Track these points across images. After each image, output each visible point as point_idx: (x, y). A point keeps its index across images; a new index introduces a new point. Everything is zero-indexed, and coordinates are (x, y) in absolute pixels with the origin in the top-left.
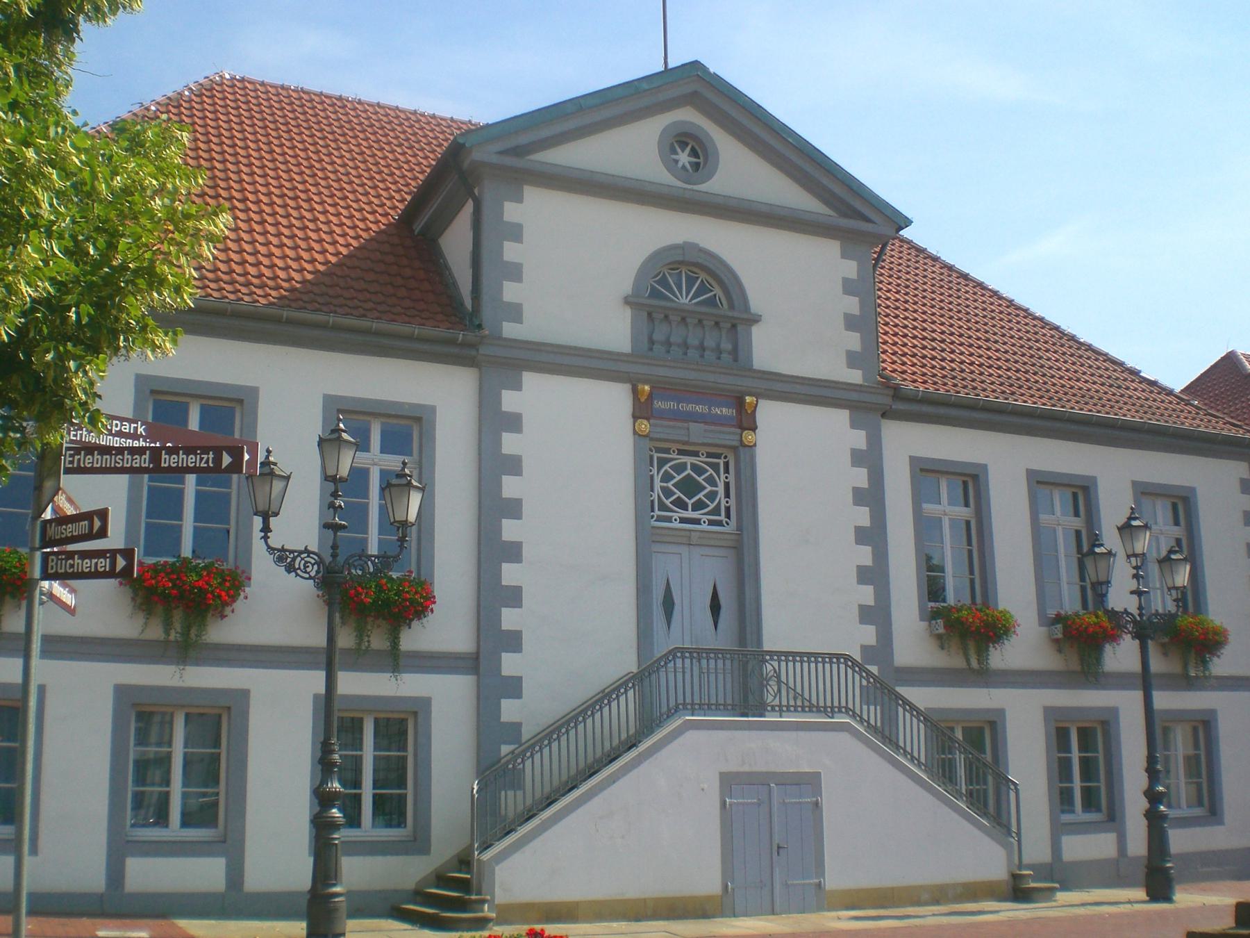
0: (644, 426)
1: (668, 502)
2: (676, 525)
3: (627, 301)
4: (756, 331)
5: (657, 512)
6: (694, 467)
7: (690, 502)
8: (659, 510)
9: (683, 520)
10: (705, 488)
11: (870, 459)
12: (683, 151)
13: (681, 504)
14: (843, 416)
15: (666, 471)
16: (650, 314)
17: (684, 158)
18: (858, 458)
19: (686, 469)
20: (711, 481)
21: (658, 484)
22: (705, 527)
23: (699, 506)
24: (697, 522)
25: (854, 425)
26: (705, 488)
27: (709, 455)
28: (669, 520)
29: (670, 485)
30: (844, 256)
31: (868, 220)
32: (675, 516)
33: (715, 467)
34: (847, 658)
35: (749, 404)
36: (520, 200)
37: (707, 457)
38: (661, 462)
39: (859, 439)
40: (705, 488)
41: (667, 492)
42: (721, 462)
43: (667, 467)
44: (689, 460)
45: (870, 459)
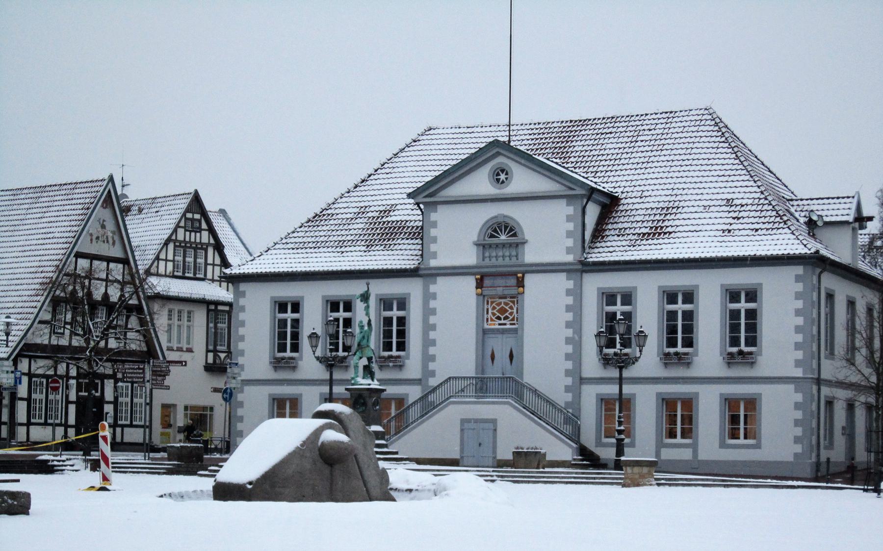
0: (479, 290)
3: (477, 244)
4: (526, 246)
7: (502, 317)
9: (500, 324)
11: (577, 293)
13: (499, 318)
14: (563, 276)
16: (484, 247)
17: (502, 177)
18: (569, 292)
20: (511, 308)
22: (508, 326)
23: (506, 318)
24: (505, 324)
25: (568, 279)
27: (511, 298)
28: (494, 324)
30: (568, 205)
31: (574, 189)
33: (513, 302)
34: (450, 378)
36: (436, 211)
38: (492, 303)
39: (570, 284)
40: (508, 311)
43: (494, 305)
44: (503, 301)
45: (577, 293)
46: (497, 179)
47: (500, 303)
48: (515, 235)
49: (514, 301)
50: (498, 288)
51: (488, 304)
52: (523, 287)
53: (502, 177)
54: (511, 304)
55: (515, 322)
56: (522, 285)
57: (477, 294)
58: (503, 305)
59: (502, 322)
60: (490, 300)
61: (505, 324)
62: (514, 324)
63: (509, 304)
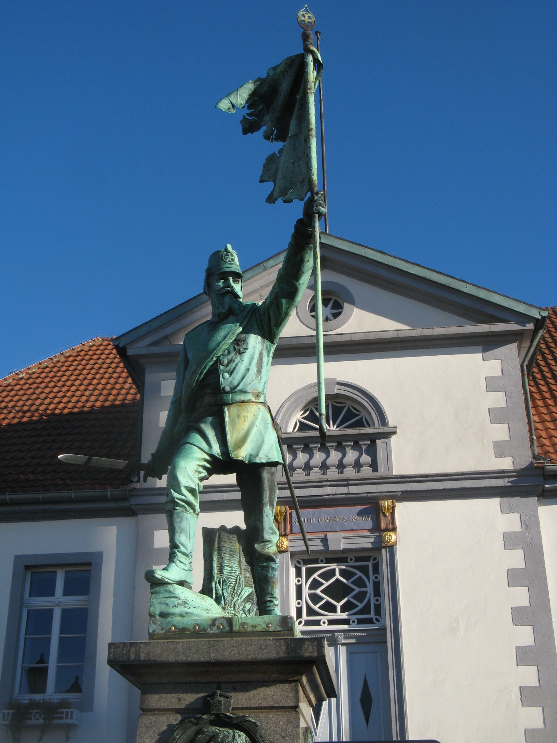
1: (316, 608)
2: (325, 627)
5: (305, 617)
6: (342, 573)
7: (339, 605)
8: (370, 613)
9: (331, 622)
12: (332, 308)
15: (315, 580)
19: (334, 575)
20: (360, 583)
21: (306, 592)
26: (353, 590)
27: (357, 559)
28: (317, 623)
29: (318, 591)
32: (323, 619)
33: (364, 570)
37: (355, 561)
38: (310, 572)
41: (315, 598)
42: (370, 564)
43: (315, 576)
46: (312, 316)
47: (332, 573)
48: (360, 424)
52: (394, 529)
58: (338, 576)
63: (354, 574)
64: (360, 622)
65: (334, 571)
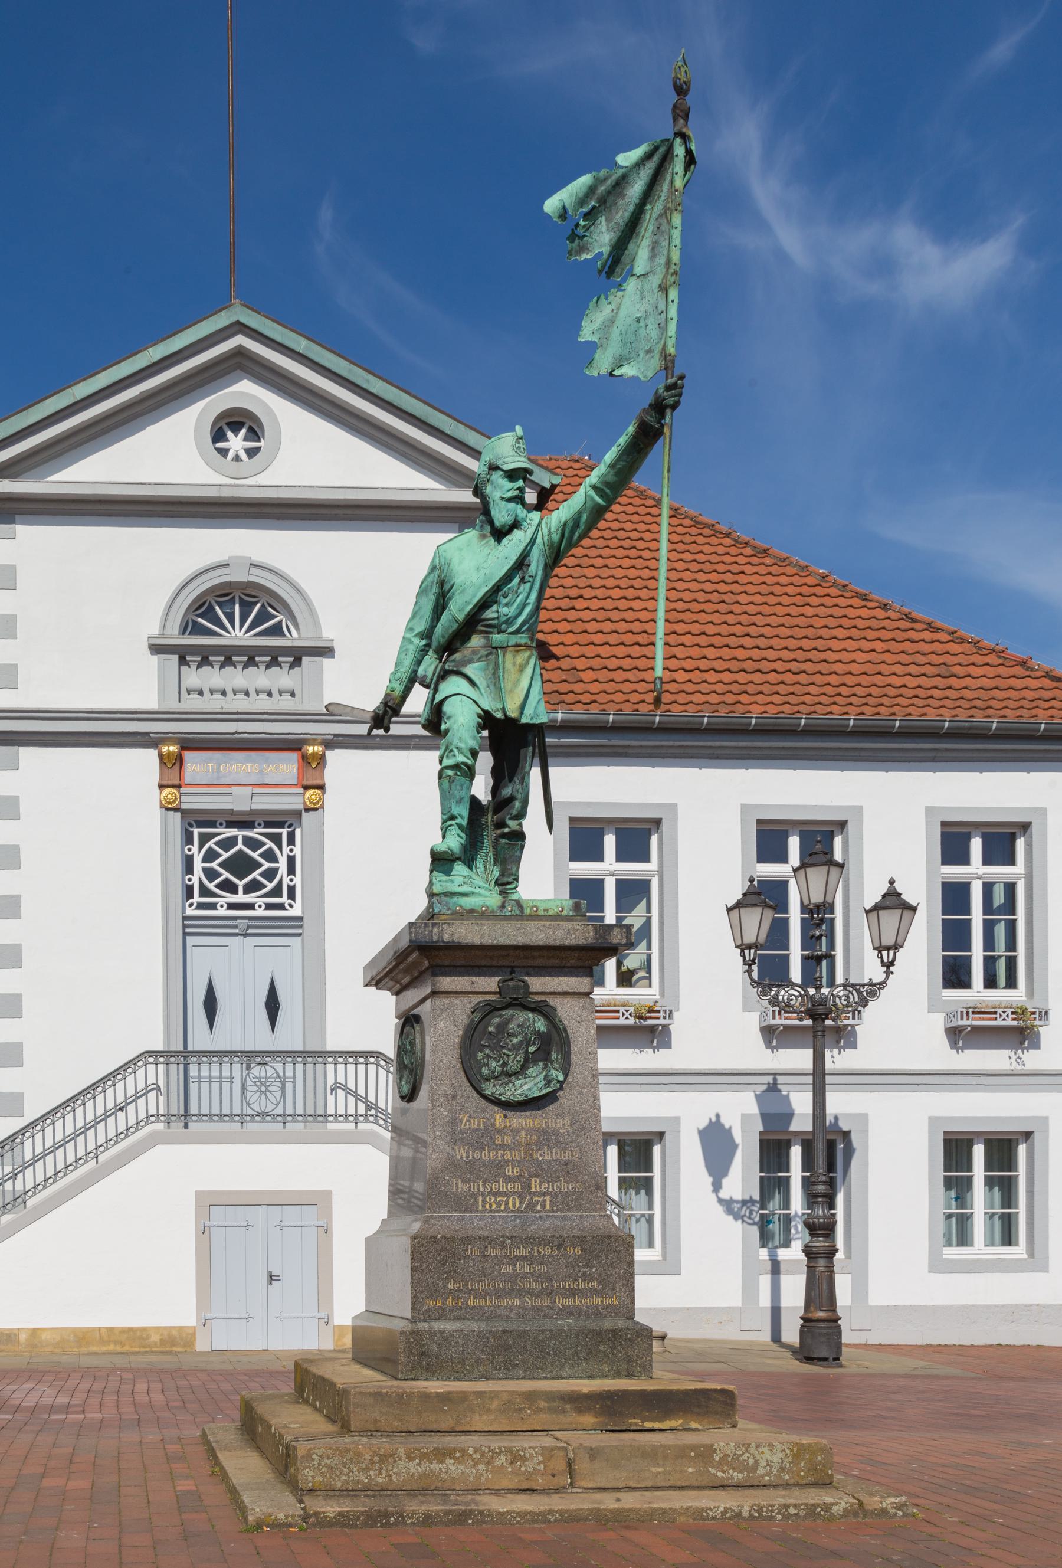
2: (222, 912)
5: (197, 898)
7: (241, 884)
9: (232, 906)
10: (261, 865)
13: (229, 887)
23: (251, 888)
24: (250, 906)
27: (268, 824)
28: (213, 906)
33: (276, 839)
35: (313, 754)
38: (204, 839)
42: (284, 832)
44: (240, 833)
47: (230, 842)
49: (280, 835)
50: (235, 790)
51: (189, 840)
53: (236, 442)
54: (270, 844)
55: (284, 899)
56: (318, 782)
57: (162, 806)
58: (240, 846)
59: (241, 898)
60: (196, 831)
61: (250, 906)
62: (281, 906)
64: (269, 906)
65: (236, 837)
